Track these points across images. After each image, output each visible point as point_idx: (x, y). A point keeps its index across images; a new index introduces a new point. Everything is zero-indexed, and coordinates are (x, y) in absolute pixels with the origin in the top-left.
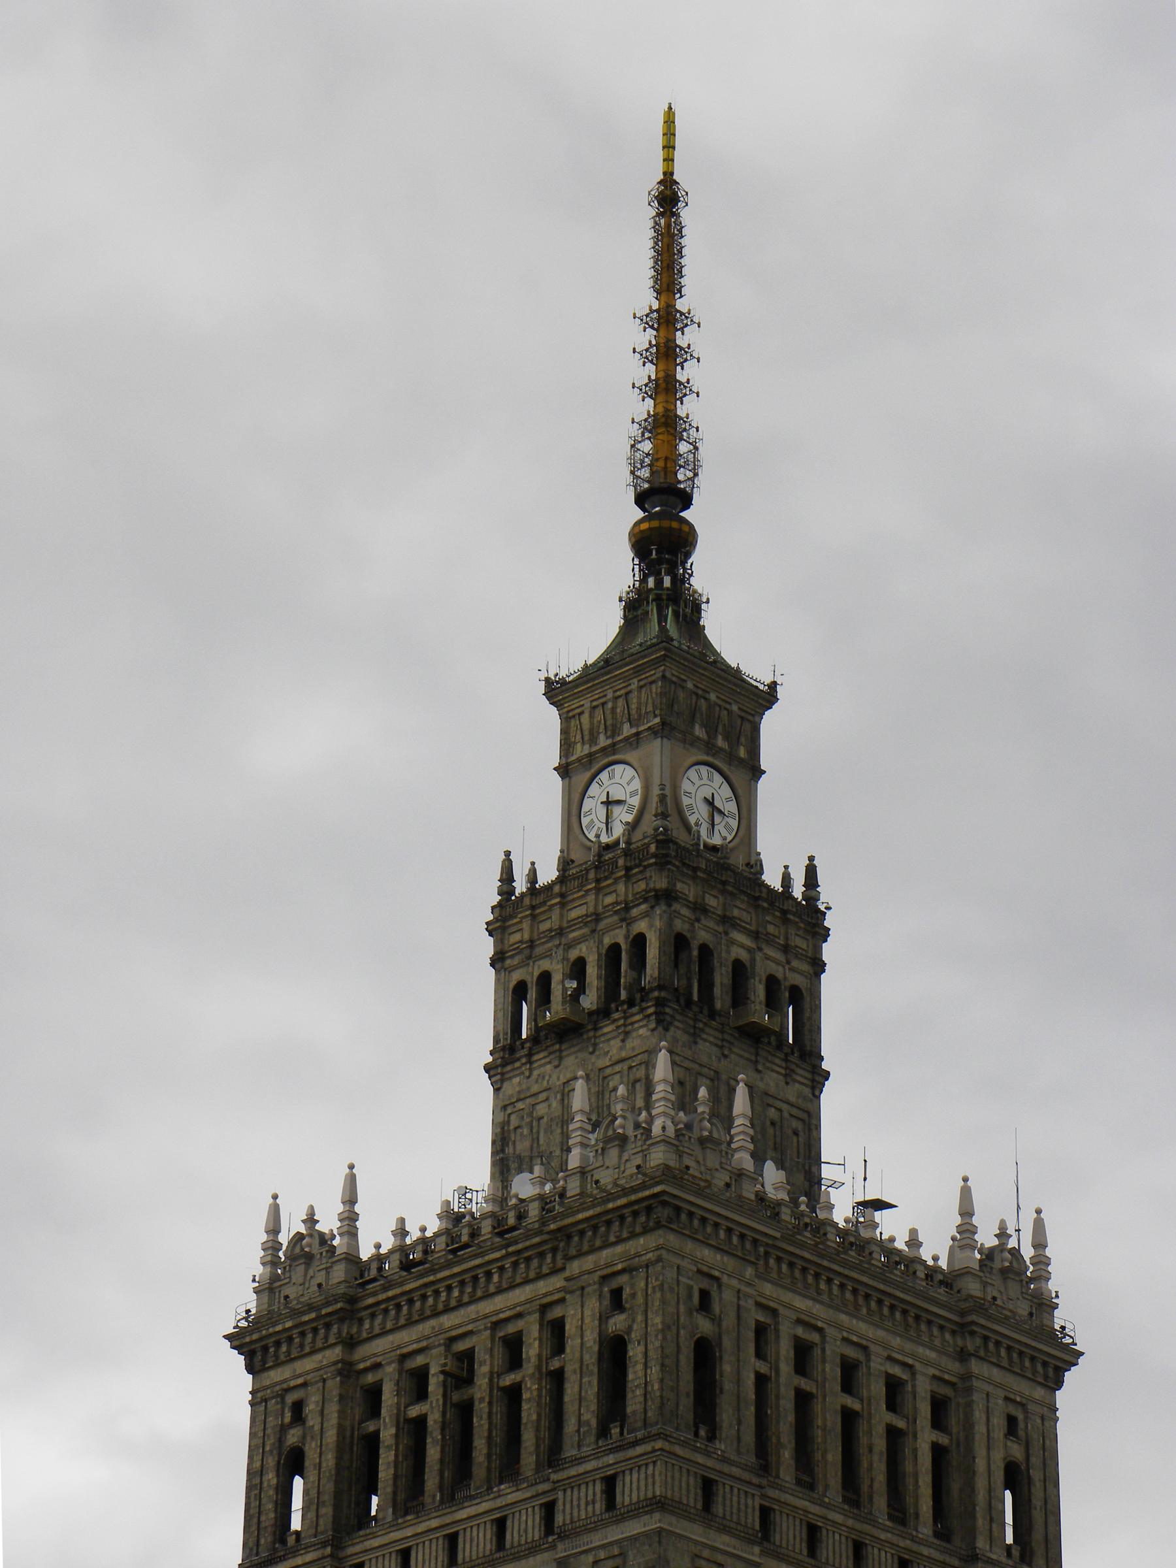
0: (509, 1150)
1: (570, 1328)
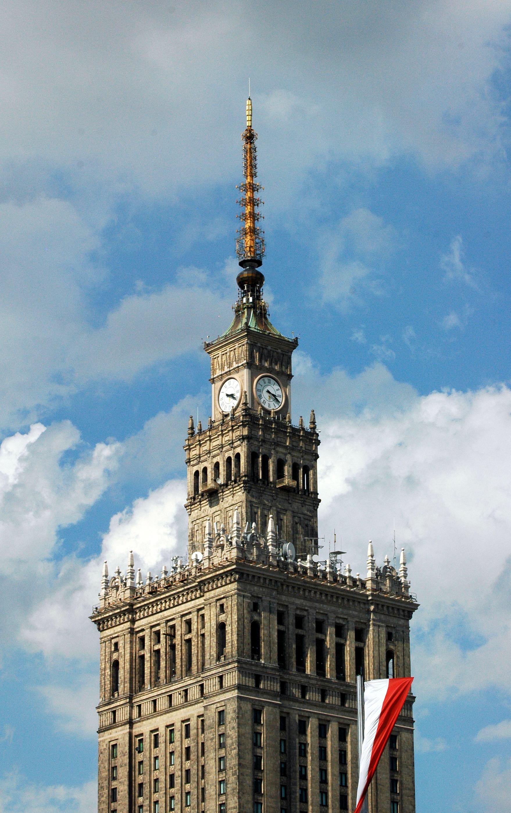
0: (195, 539)
1: (206, 618)
